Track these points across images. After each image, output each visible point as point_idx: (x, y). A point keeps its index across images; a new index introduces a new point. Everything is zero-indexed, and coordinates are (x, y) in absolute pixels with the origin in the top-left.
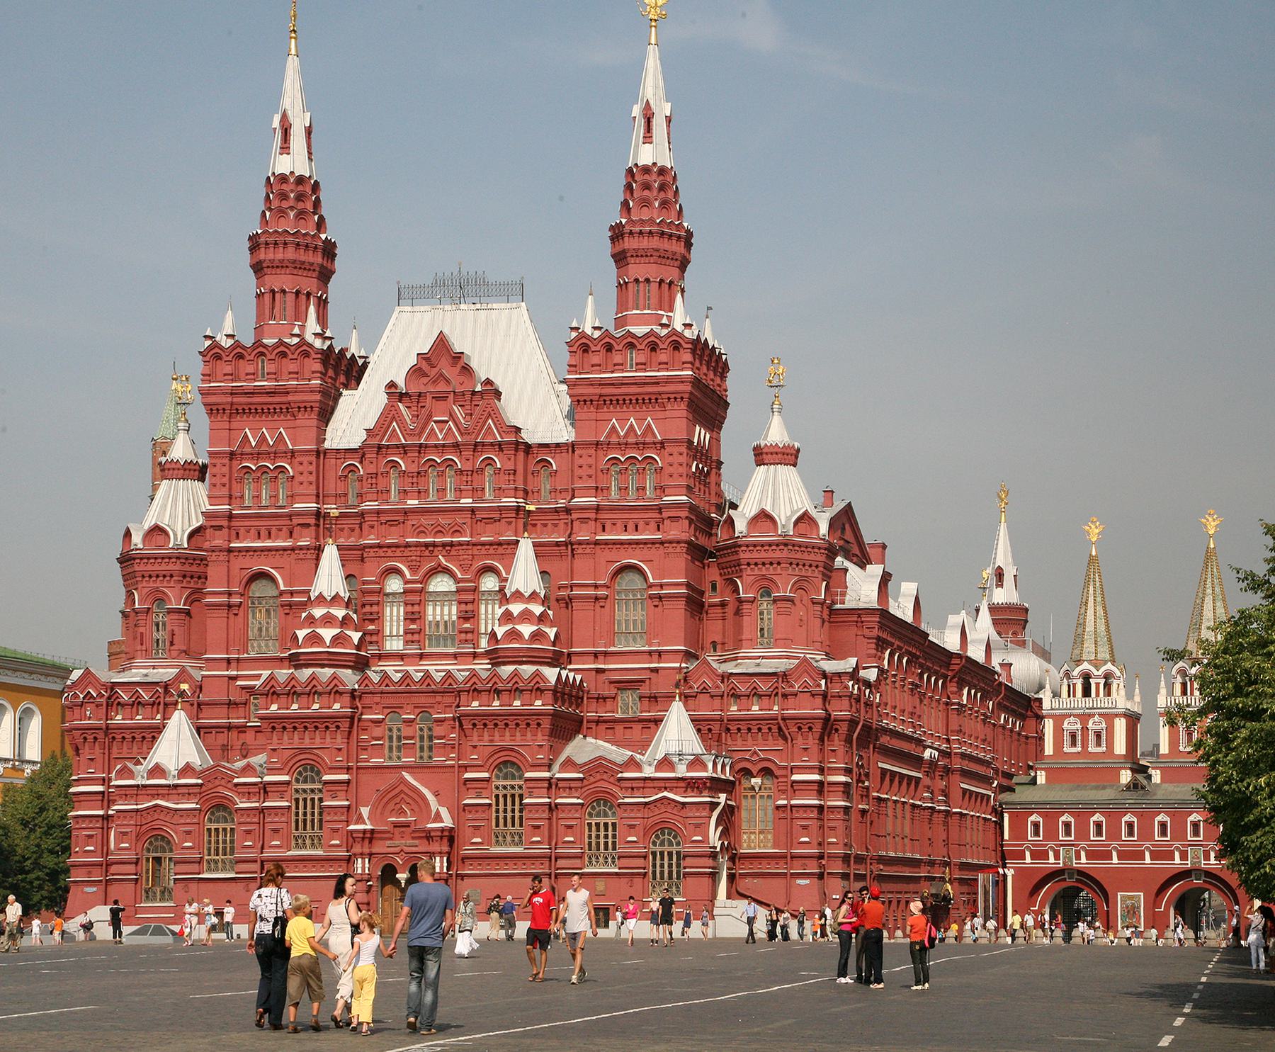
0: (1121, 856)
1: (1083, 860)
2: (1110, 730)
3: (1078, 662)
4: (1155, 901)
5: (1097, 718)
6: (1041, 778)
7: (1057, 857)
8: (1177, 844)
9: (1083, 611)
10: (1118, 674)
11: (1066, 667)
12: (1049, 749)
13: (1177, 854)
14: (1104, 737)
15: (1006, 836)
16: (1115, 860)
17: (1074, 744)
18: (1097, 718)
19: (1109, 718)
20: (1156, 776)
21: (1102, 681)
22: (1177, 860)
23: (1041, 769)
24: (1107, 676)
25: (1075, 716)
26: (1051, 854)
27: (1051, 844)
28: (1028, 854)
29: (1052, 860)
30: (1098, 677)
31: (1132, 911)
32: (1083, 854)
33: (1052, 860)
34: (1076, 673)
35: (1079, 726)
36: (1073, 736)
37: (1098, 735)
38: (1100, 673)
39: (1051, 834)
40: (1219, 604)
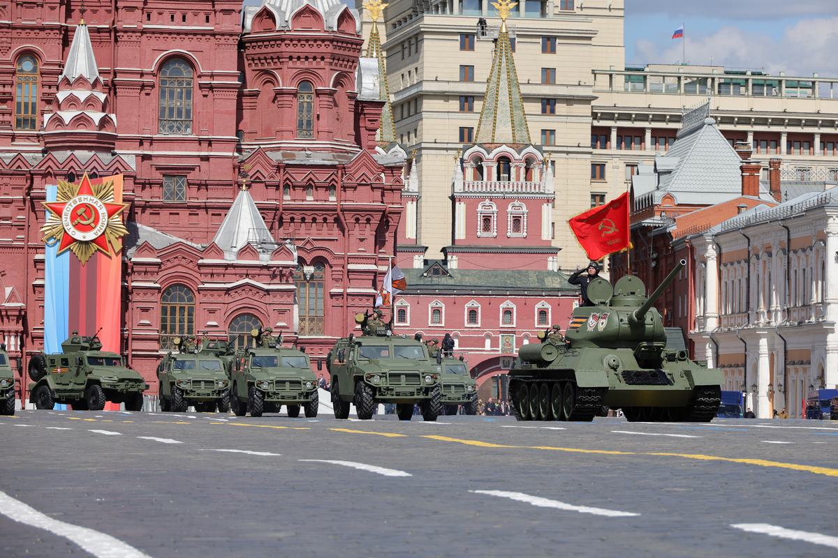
8: (488, 331)
13: (488, 342)
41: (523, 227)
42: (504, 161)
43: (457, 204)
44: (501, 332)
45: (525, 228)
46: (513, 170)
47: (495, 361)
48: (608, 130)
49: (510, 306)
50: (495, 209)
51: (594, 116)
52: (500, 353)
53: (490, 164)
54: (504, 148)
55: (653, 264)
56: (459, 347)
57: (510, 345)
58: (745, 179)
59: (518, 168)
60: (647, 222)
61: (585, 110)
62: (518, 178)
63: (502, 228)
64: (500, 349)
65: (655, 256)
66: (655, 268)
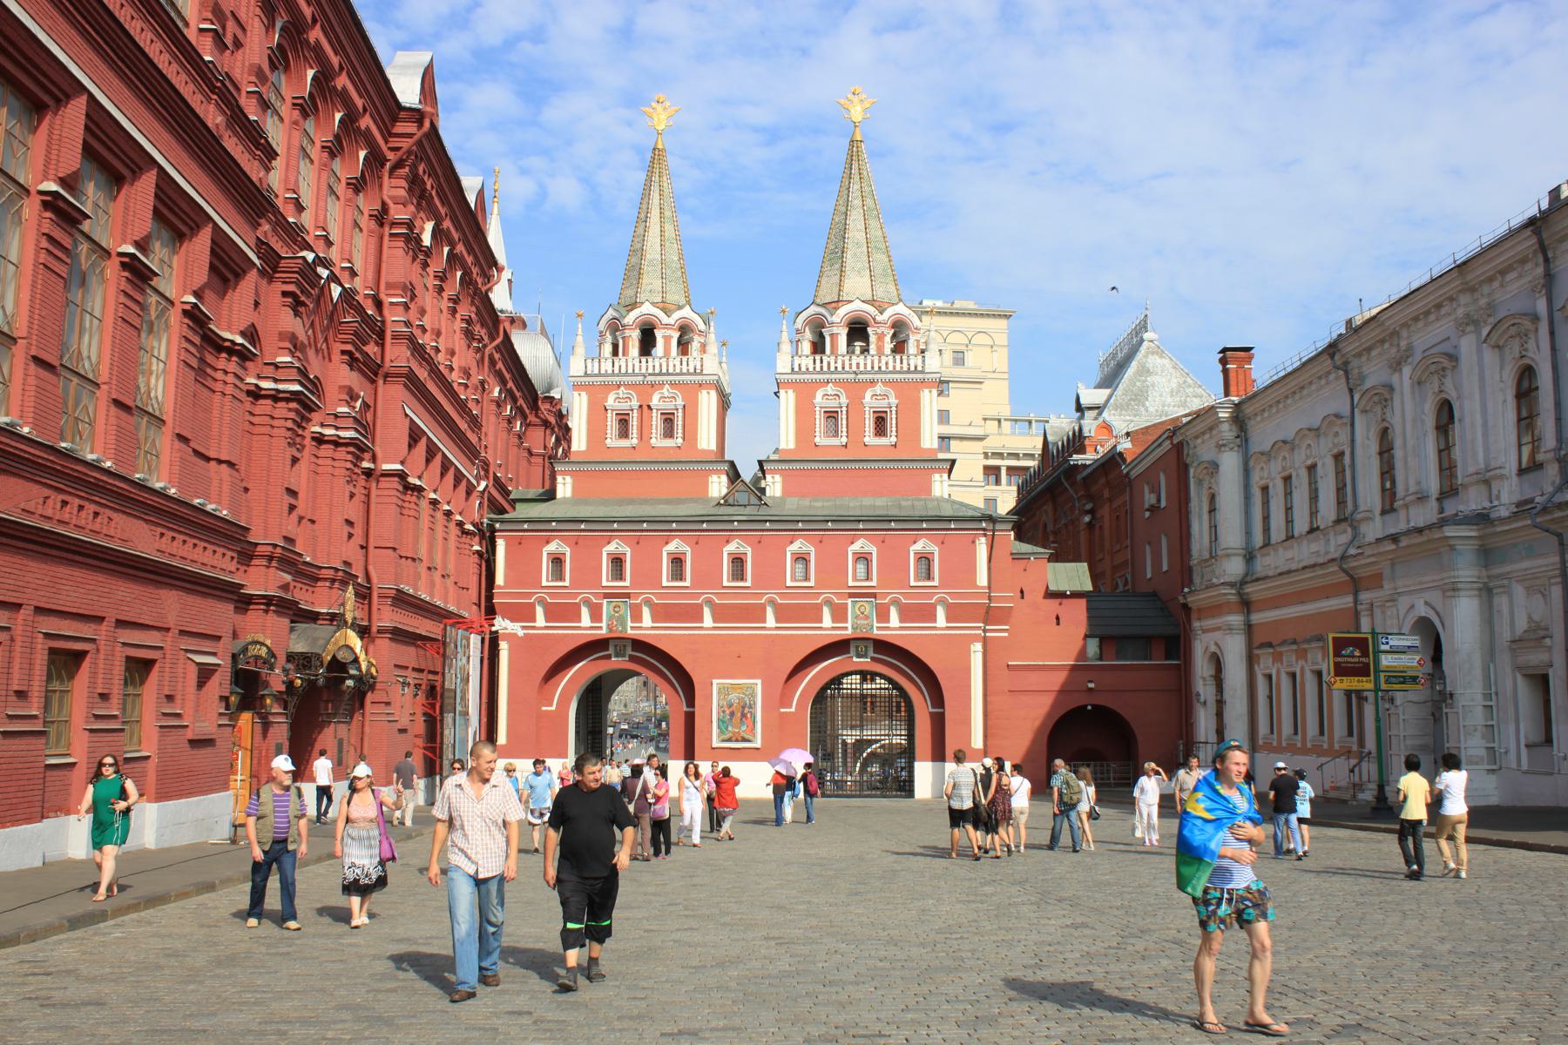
0: (720, 614)
2: (690, 410)
3: (633, 306)
4: (783, 695)
5: (666, 391)
6: (564, 487)
7: (596, 615)
8: (827, 593)
9: (640, 230)
10: (702, 327)
11: (611, 313)
12: (579, 442)
13: (826, 612)
14: (679, 422)
15: (500, 579)
17: (624, 432)
19: (690, 390)
20: (774, 486)
21: (676, 335)
23: (564, 473)
24: (685, 330)
25: (627, 386)
26: (585, 612)
27: (586, 593)
28: (539, 611)
29: (586, 620)
31: (739, 713)
32: (646, 613)
33: (586, 620)
34: (630, 318)
35: (635, 403)
36: (624, 422)
37: (668, 420)
38: (671, 321)
40: (873, 223)
42: (858, 331)
44: (851, 595)
46: (873, 339)
48: (997, 469)
49: (866, 549)
50: (844, 400)
51: (986, 455)
52: (849, 632)
53: (835, 330)
54: (857, 305)
55: (1087, 519)
56: (778, 620)
57: (867, 618)
58: (1232, 375)
59: (881, 337)
60: (1077, 458)
61: (978, 447)
62: (880, 352)
63: (855, 431)
64: (849, 625)
65: (1089, 507)
66: (1090, 525)
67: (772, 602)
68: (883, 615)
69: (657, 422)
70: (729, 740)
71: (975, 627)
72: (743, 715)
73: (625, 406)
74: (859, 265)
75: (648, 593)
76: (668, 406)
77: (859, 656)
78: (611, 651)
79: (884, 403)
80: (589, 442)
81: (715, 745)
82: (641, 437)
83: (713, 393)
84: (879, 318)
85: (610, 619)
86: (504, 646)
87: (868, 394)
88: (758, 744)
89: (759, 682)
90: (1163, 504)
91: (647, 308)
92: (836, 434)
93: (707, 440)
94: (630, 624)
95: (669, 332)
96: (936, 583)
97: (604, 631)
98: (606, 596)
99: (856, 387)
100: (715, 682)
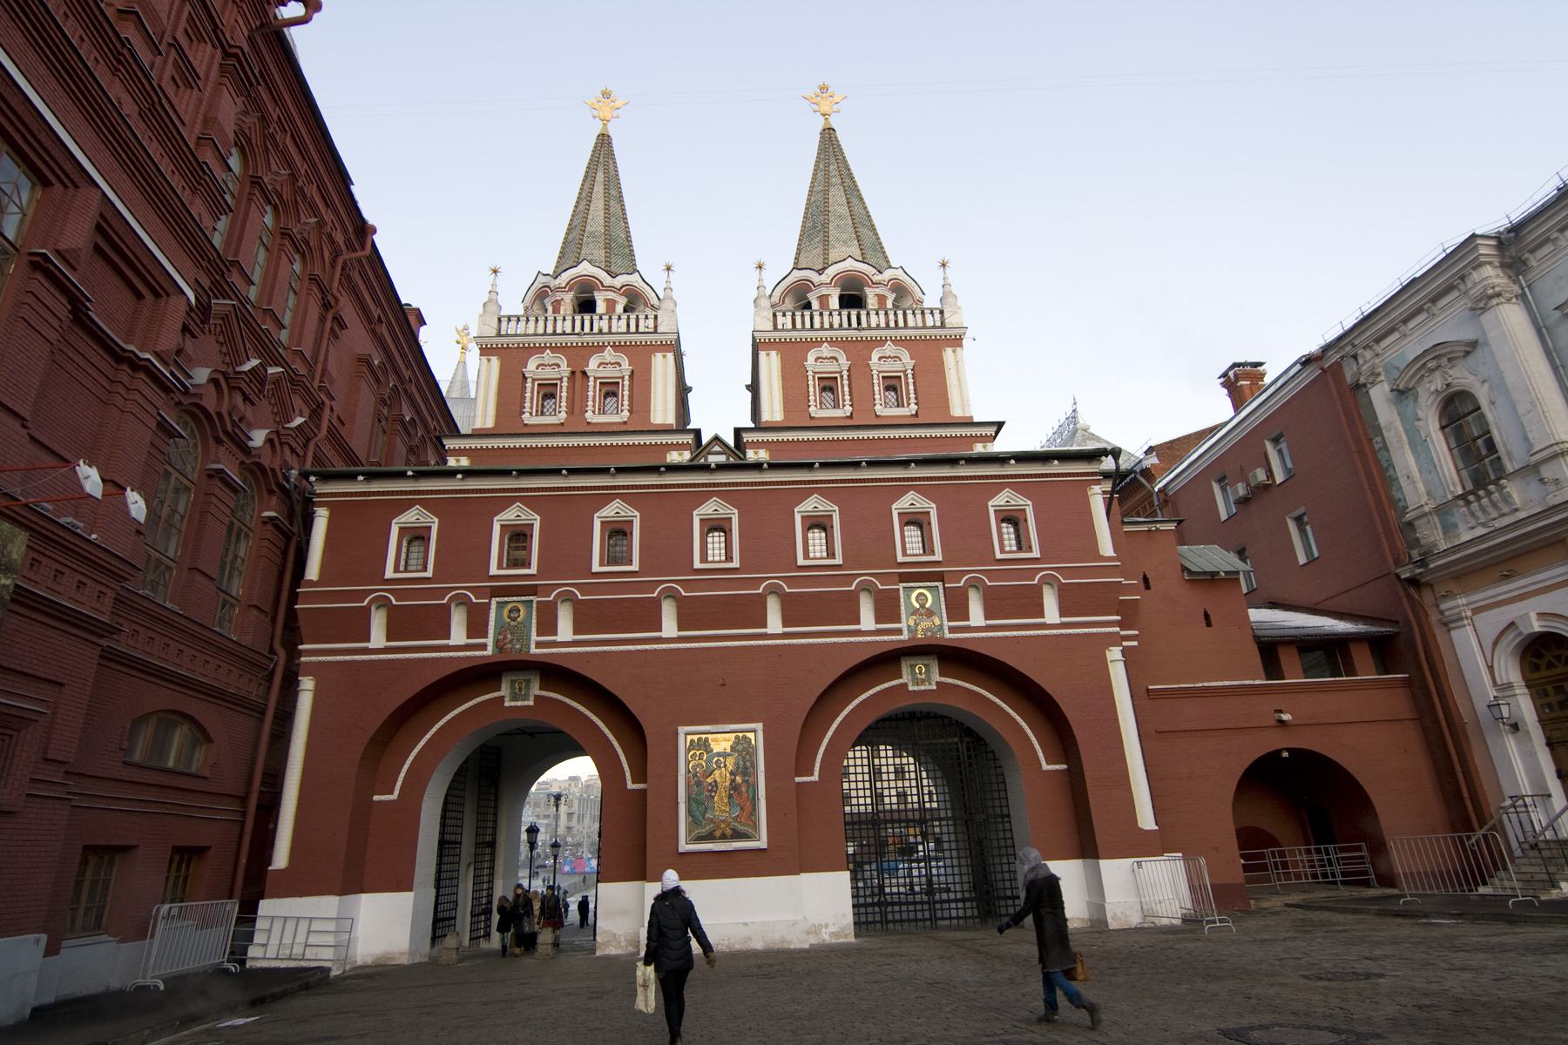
1: (565, 631)
5: (609, 355)
7: (476, 626)
8: (864, 575)
15: (313, 571)
16: (669, 628)
18: (609, 355)
19: (640, 354)
22: (867, 620)
27: (462, 587)
29: (458, 635)
30: (610, 288)
33: (458, 635)
35: (565, 370)
38: (619, 281)
39: (463, 555)
41: (908, 393)
43: (762, 355)
44: (904, 578)
45: (912, 396)
47: (888, 660)
50: (844, 362)
53: (824, 291)
63: (862, 398)
67: (774, 590)
68: (957, 608)
69: (593, 390)
70: (709, 837)
71: (1104, 623)
72: (734, 787)
73: (549, 373)
74: (844, 236)
75: (568, 584)
76: (610, 373)
77: (917, 682)
78: (505, 691)
79: (897, 366)
80: (497, 416)
81: (684, 846)
82: (570, 412)
83: (670, 356)
84: (877, 278)
85: (500, 630)
86: (307, 684)
87: (875, 356)
88: (762, 843)
89: (759, 726)
90: (1279, 477)
91: (585, 268)
92: (837, 406)
93: (662, 411)
94: (534, 638)
95: (611, 295)
96: (1036, 553)
97: (489, 651)
98: (496, 592)
99: (859, 350)
100: (682, 730)
